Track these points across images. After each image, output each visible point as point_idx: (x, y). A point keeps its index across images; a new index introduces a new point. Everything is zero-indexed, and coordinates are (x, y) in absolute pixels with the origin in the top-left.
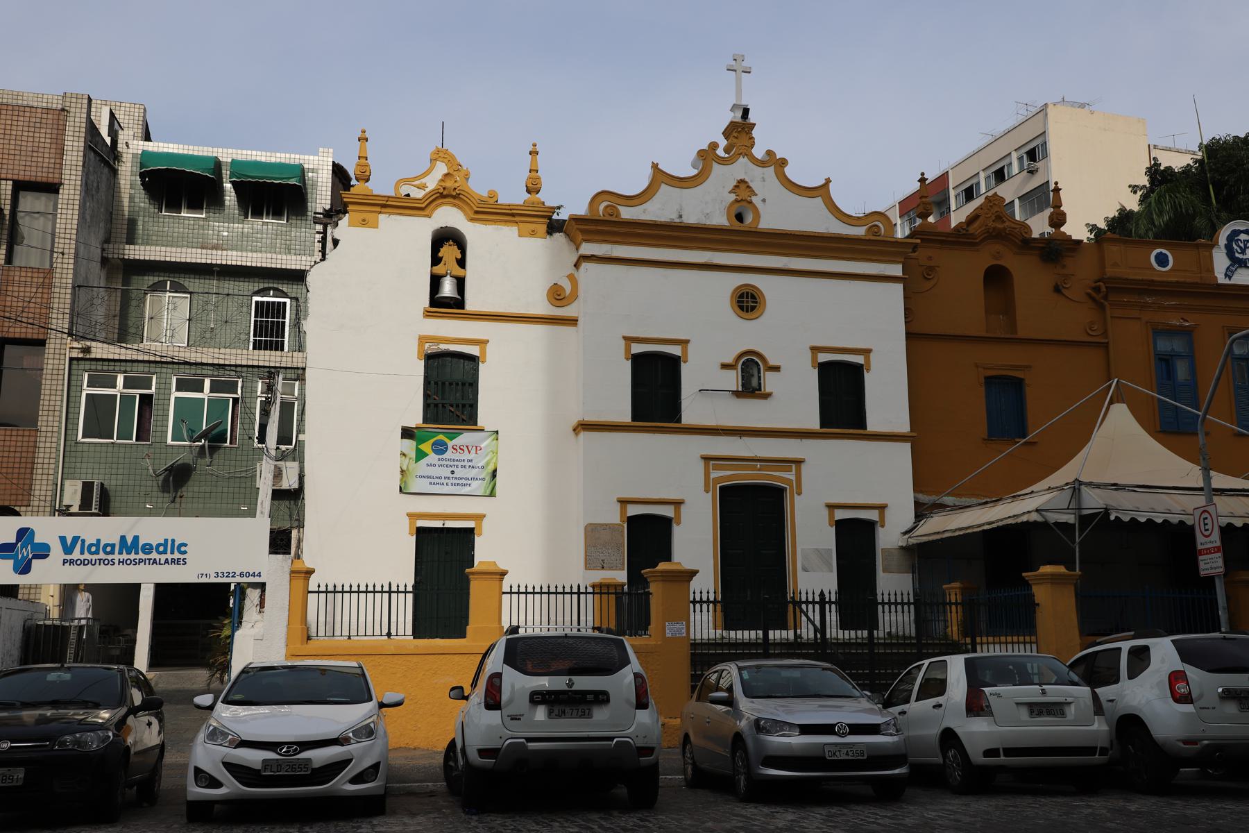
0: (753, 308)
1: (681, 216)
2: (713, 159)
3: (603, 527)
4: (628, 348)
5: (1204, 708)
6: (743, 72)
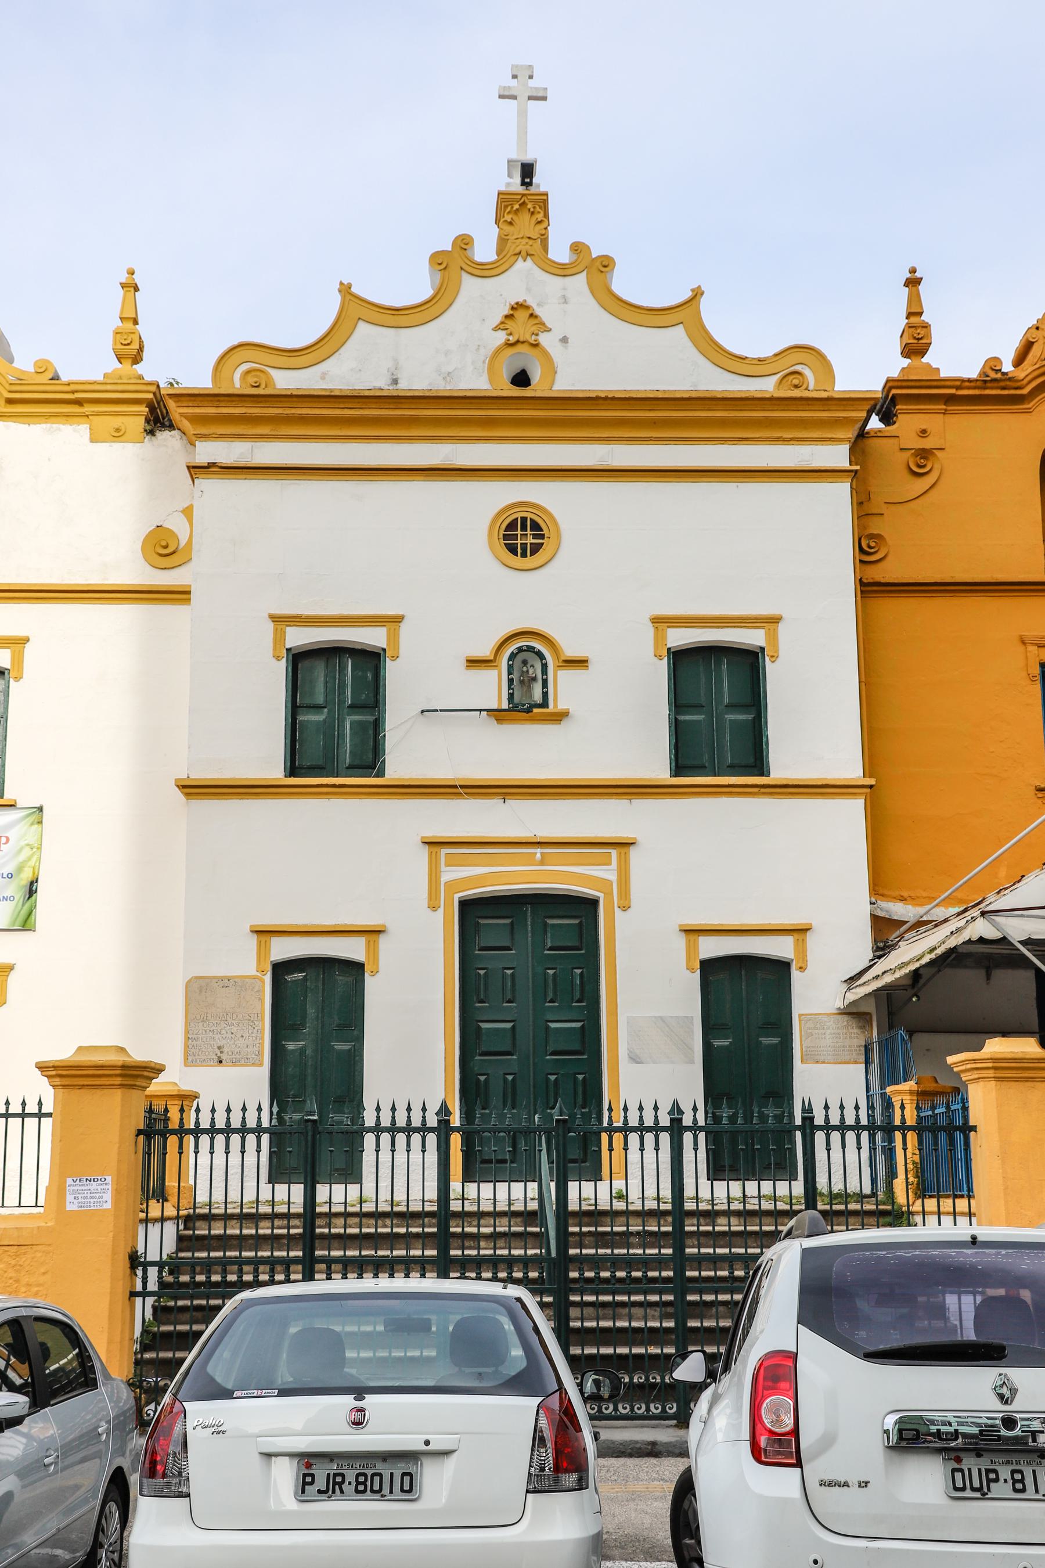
0: (536, 549)
1: (395, 382)
2: (462, 268)
3: (221, 983)
4: (279, 638)
5: (831, 1484)
6: (530, 98)
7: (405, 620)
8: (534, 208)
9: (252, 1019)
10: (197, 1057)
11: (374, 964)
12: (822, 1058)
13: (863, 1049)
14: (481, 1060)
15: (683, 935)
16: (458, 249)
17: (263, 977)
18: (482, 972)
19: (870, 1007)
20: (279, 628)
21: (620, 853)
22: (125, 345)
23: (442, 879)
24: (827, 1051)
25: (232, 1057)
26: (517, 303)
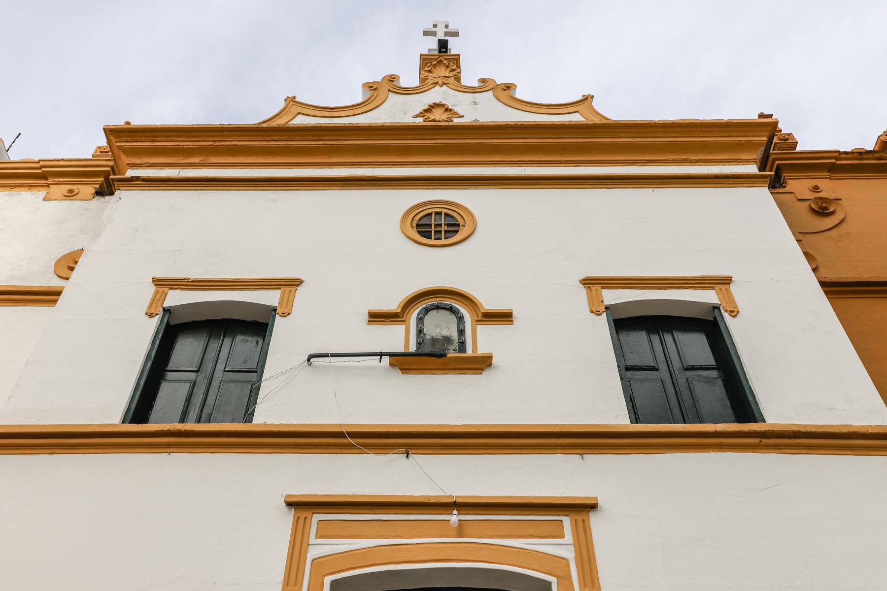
2: (389, 90)
7: (303, 284)
8: (449, 64)
16: (387, 81)
20: (161, 290)
22: (103, 152)
26: (434, 104)
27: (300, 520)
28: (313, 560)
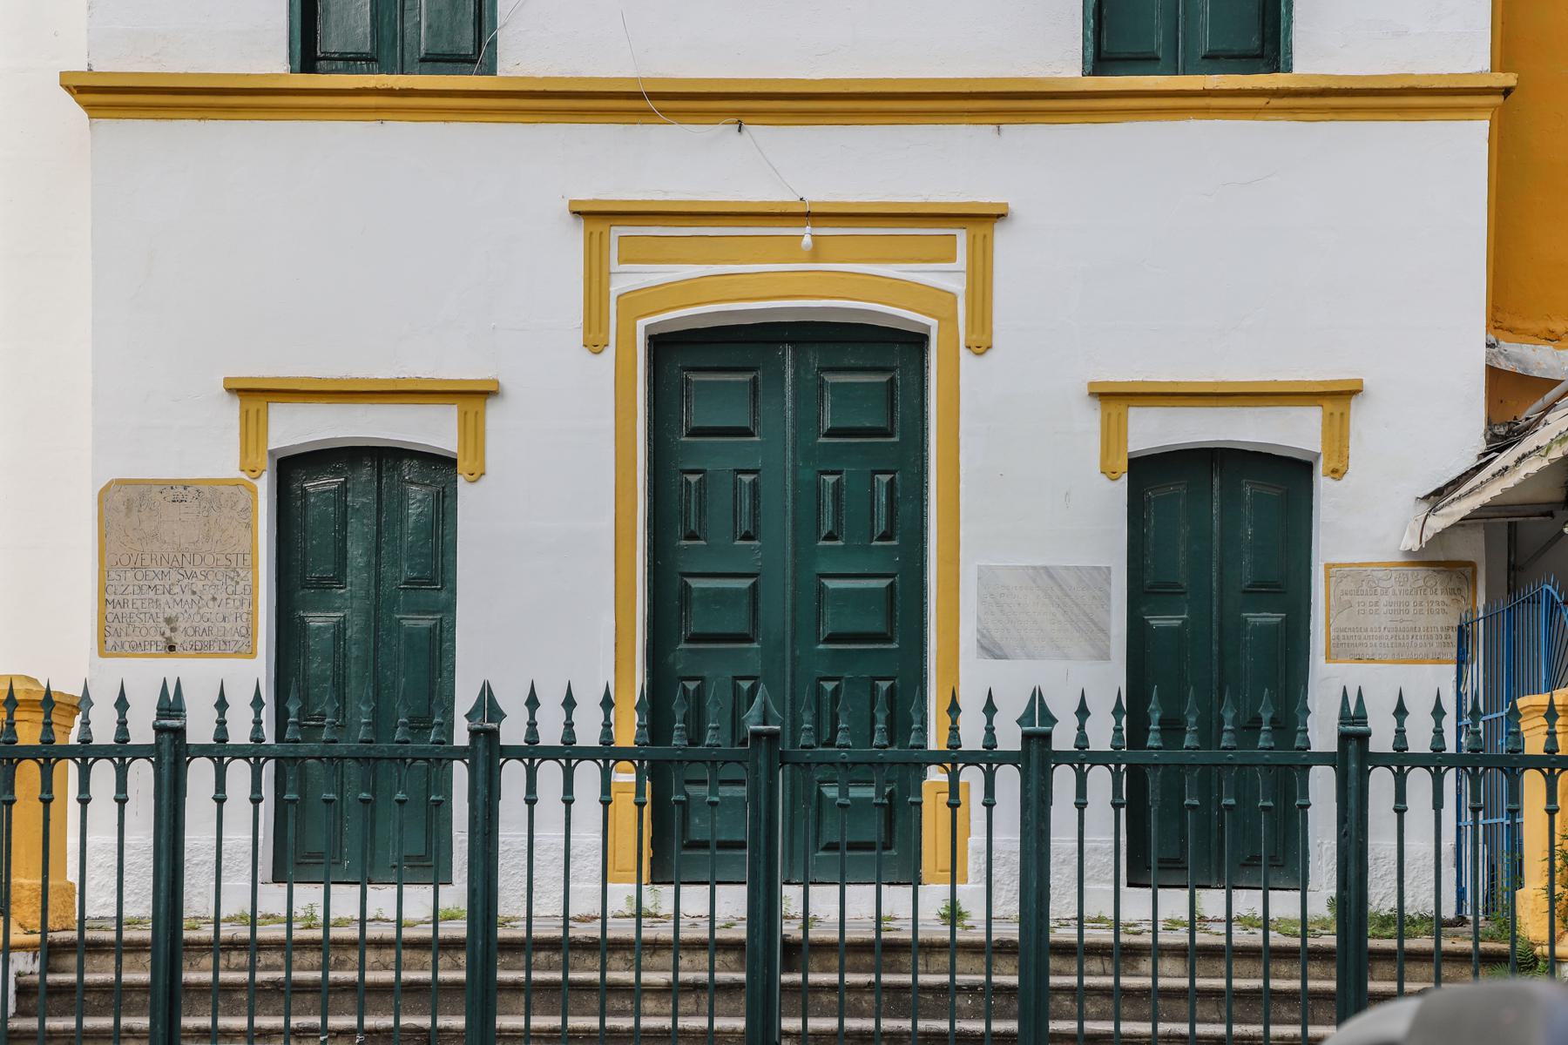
3: (170, 495)
9: (234, 565)
10: (124, 638)
11: (476, 459)
12: (1369, 652)
13: (1454, 635)
14: (690, 650)
15: (1097, 403)
17: (255, 482)
18: (693, 478)
19: (1472, 548)
21: (974, 236)
23: (612, 289)
24: (1380, 637)
25: (194, 638)
27: (594, 236)
28: (619, 297)
